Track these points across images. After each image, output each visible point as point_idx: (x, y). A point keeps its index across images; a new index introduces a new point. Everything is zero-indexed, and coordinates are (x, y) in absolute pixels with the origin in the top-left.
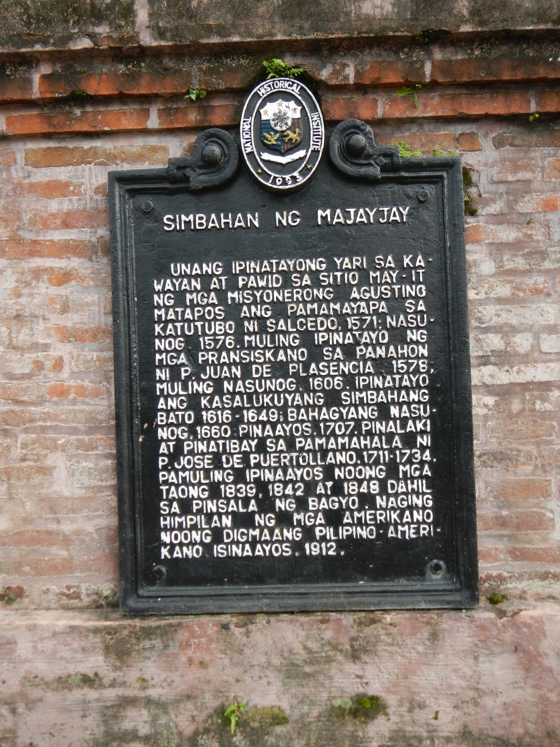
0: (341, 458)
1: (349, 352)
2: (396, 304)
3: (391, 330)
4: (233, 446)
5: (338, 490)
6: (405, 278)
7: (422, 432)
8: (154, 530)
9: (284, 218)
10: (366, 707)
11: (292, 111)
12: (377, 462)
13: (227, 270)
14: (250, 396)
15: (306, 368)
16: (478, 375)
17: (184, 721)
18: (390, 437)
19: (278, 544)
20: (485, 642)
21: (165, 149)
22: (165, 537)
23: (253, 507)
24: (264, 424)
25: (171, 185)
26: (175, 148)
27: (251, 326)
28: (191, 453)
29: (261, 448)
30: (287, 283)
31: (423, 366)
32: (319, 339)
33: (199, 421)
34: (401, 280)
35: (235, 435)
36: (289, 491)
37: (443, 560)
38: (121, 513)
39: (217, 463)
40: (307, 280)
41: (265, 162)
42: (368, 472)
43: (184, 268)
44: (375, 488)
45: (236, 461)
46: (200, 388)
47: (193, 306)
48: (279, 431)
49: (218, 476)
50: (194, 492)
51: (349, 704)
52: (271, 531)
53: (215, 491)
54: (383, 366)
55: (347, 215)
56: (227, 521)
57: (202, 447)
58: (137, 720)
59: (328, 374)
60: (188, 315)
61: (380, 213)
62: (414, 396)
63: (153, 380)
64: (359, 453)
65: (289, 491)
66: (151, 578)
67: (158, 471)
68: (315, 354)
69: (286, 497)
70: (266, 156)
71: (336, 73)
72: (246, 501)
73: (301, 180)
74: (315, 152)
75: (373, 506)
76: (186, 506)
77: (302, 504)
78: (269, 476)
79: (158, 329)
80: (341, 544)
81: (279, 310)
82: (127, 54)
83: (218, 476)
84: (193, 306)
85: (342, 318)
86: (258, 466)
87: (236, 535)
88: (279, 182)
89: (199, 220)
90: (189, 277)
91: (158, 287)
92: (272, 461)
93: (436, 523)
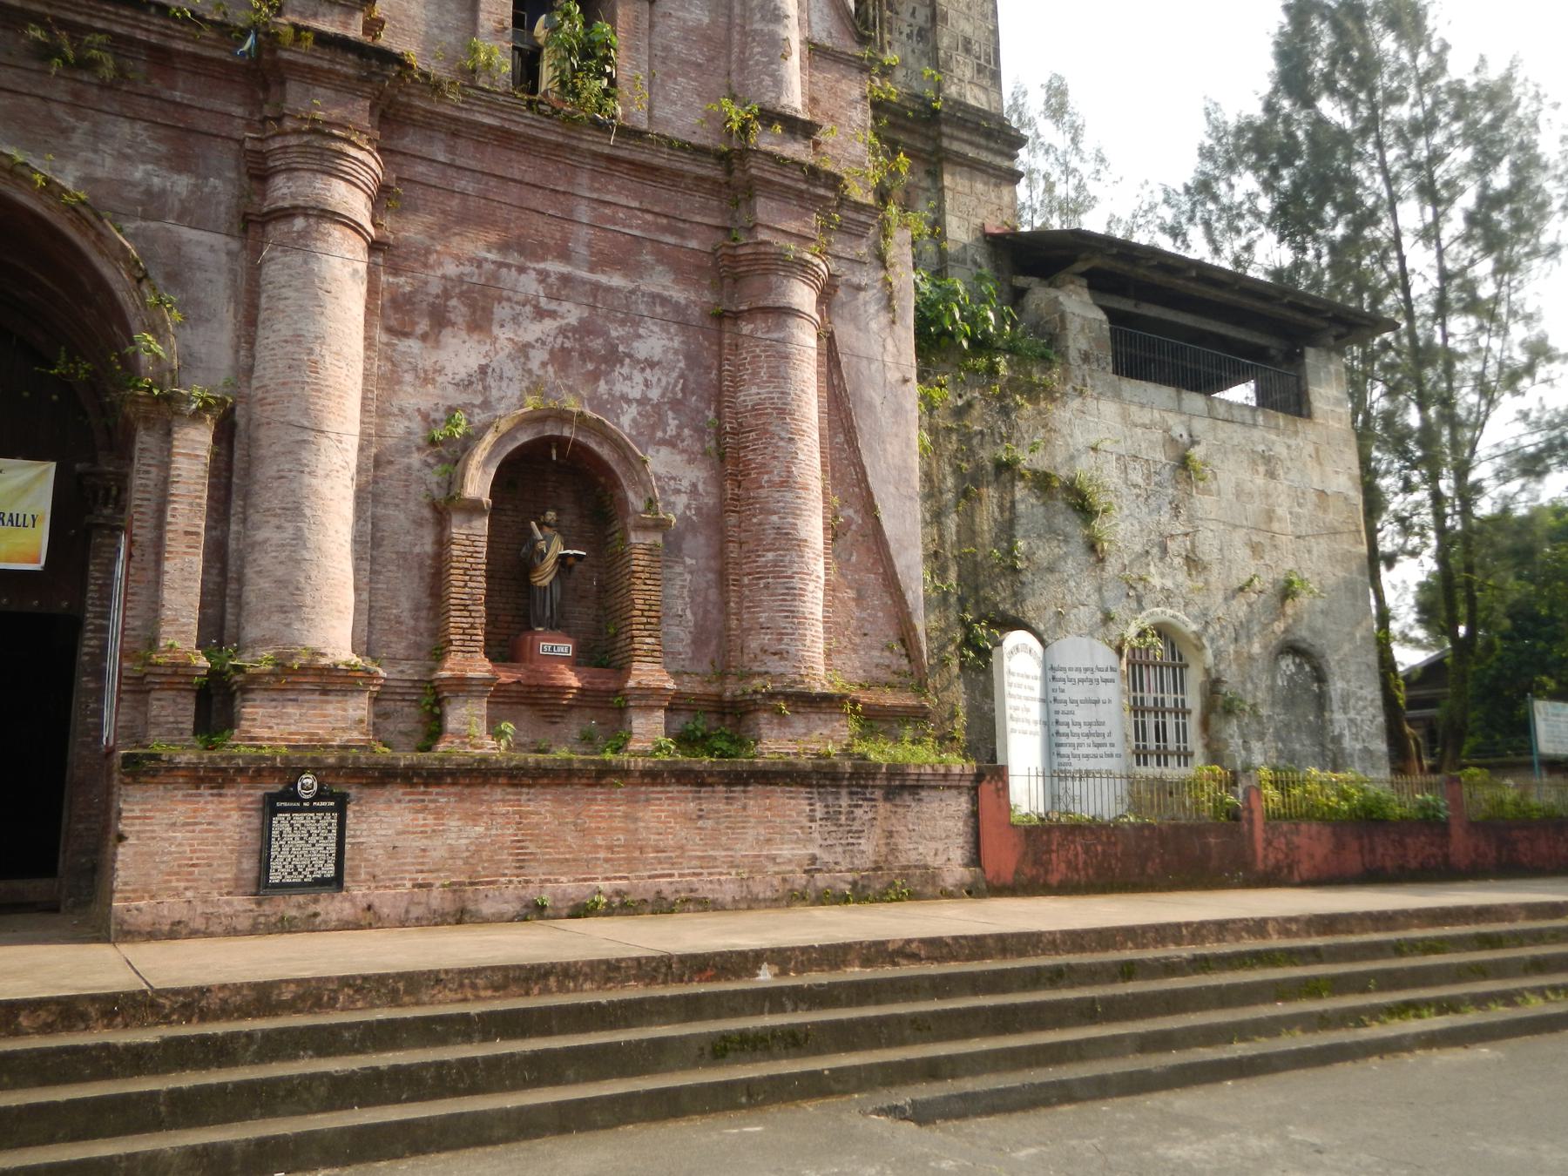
10: (316, 915)
17: (273, 920)
20: (345, 899)
25: (281, 796)
26: (280, 787)
37: (336, 883)
58: (262, 919)
59: (313, 840)
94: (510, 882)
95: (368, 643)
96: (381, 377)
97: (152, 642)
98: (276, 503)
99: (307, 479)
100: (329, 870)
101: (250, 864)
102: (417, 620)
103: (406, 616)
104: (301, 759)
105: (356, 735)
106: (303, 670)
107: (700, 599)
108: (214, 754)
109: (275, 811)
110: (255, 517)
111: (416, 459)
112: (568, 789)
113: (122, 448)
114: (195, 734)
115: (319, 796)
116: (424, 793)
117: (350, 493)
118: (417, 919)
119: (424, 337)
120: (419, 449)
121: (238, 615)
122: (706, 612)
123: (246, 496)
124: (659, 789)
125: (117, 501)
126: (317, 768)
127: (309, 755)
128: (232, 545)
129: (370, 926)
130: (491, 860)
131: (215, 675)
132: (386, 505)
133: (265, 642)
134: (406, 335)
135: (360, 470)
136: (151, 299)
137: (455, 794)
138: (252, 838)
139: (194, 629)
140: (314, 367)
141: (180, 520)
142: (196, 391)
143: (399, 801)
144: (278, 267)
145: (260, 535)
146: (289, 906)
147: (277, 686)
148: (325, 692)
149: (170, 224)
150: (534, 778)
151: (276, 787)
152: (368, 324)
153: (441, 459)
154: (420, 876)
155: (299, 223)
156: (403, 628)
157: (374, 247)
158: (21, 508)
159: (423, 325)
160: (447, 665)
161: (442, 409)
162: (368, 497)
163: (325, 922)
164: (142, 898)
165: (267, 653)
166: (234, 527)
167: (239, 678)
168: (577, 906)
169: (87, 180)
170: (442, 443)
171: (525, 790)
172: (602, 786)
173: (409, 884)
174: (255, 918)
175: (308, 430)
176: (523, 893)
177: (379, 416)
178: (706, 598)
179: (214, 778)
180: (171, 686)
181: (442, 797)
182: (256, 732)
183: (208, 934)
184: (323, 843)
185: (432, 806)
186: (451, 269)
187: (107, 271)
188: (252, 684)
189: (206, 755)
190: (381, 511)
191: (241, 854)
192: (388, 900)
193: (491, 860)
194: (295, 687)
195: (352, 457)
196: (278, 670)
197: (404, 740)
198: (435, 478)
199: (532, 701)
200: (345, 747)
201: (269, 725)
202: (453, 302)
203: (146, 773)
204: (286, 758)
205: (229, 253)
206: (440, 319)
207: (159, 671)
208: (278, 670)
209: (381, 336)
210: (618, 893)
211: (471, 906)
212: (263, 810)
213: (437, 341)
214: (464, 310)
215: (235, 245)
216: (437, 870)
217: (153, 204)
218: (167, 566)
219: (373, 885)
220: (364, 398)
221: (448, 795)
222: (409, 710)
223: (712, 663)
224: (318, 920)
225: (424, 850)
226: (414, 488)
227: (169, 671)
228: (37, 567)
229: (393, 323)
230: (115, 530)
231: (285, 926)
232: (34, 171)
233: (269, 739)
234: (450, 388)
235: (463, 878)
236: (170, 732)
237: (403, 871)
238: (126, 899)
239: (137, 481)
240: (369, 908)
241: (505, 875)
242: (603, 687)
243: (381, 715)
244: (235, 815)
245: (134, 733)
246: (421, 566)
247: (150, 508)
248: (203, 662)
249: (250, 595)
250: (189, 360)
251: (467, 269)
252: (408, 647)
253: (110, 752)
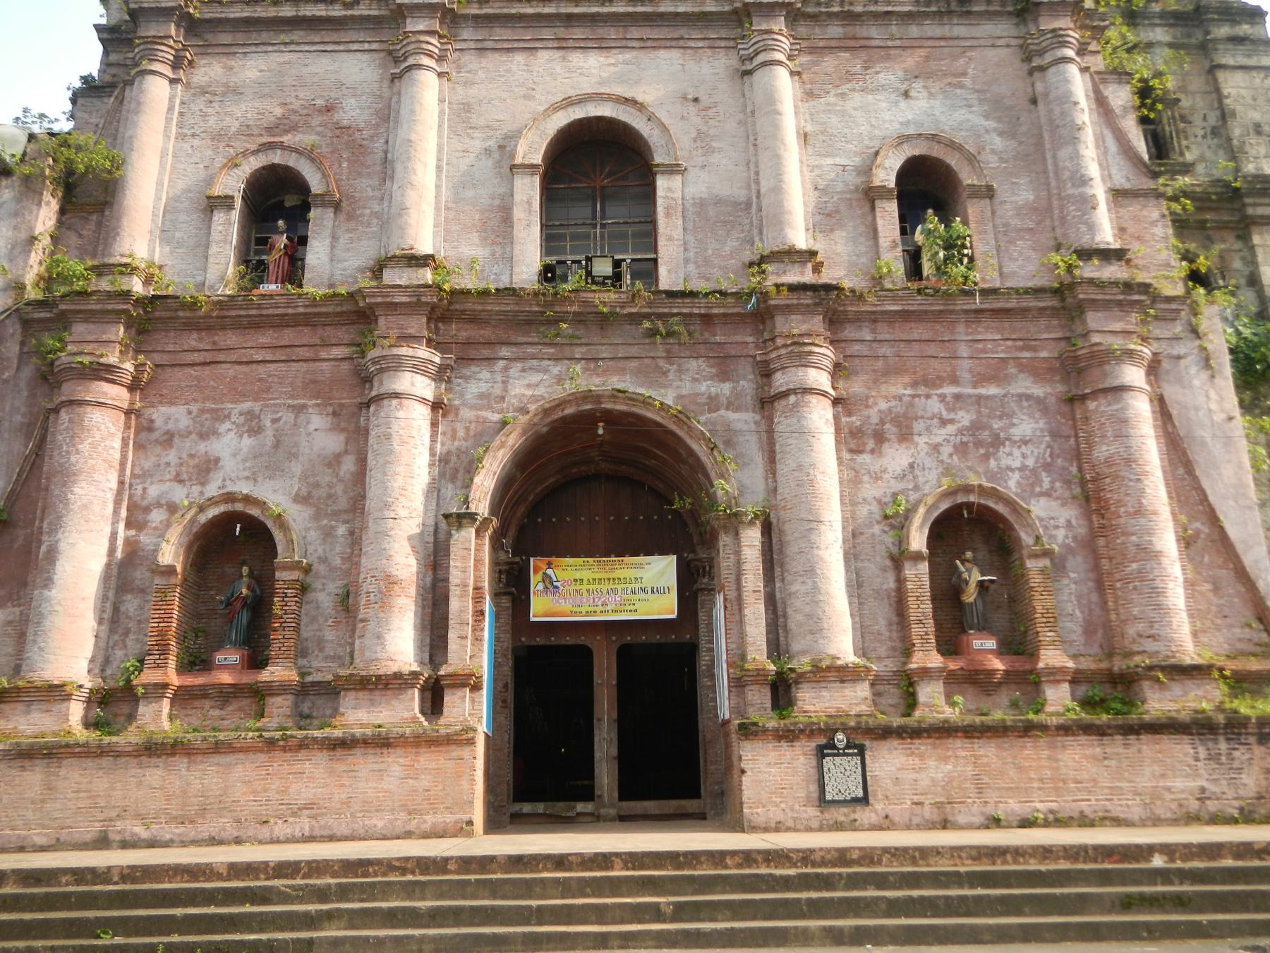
10: (855, 820)
19: (841, 798)
37: (864, 800)
59: (848, 773)
82: (820, 729)
95: (863, 649)
96: (850, 481)
97: (743, 657)
98: (800, 568)
99: (815, 551)
100: (860, 794)
101: (814, 788)
102: (890, 631)
103: (884, 630)
105: (864, 708)
106: (829, 668)
107: (1084, 602)
108: (787, 722)
109: (824, 756)
110: (788, 578)
111: (877, 529)
113: (710, 541)
115: (848, 747)
117: (841, 557)
119: (872, 451)
120: (878, 522)
121: (786, 637)
122: (1091, 610)
123: (782, 565)
125: (709, 574)
126: (845, 729)
127: (839, 721)
128: (778, 595)
129: (888, 829)
130: (959, 787)
131: (779, 674)
132: (862, 561)
133: (804, 652)
134: (861, 452)
135: (844, 541)
136: (720, 459)
138: (813, 772)
139: (764, 647)
140: (812, 483)
141: (750, 584)
142: (749, 507)
144: (782, 424)
145: (794, 588)
146: (840, 814)
148: (842, 681)
149: (722, 412)
150: (981, 732)
151: (823, 741)
152: (838, 451)
153: (892, 527)
155: (792, 399)
157: (836, 402)
158: (661, 583)
159: (871, 444)
160: (914, 660)
161: (889, 495)
162: (851, 556)
165: (806, 659)
166: (777, 585)
167: (793, 675)
169: (680, 397)
170: (892, 517)
175: (813, 522)
177: (852, 505)
179: (788, 736)
180: (756, 682)
181: (922, 745)
182: (807, 708)
183: (796, 830)
184: (854, 776)
186: (883, 405)
187: (695, 447)
188: (801, 678)
189: (782, 722)
190: (860, 565)
191: (808, 781)
192: (898, 812)
193: (959, 787)
194: (824, 680)
195: (838, 534)
197: (893, 710)
198: (890, 540)
199: (973, 680)
200: (859, 716)
201: (815, 703)
202: (887, 426)
204: (826, 723)
205: (755, 423)
206: (880, 438)
209: (846, 456)
210: (1052, 812)
211: (950, 818)
213: (880, 453)
214: (894, 430)
215: (758, 417)
217: (713, 403)
218: (746, 612)
220: (841, 496)
222: (893, 690)
223: (1101, 646)
224: (857, 824)
226: (878, 547)
228: (674, 616)
229: (853, 446)
230: (711, 591)
231: (838, 827)
232: (654, 400)
234: (892, 481)
235: (942, 799)
236: (759, 709)
239: (724, 564)
240: (887, 817)
243: (877, 694)
244: (802, 758)
245: (738, 710)
246: (889, 597)
247: (732, 578)
248: (772, 667)
249: (792, 625)
250: (742, 489)
251: (893, 403)
253: (726, 723)
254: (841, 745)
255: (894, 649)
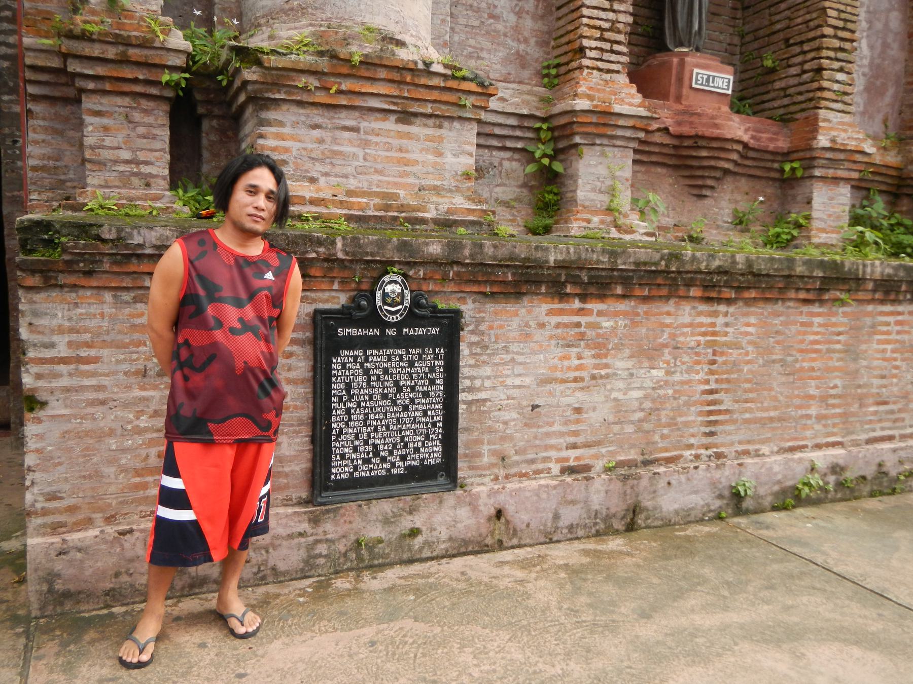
0: (408, 433)
1: (413, 389)
2: (432, 369)
3: (430, 379)
4: (364, 430)
5: (406, 446)
6: (436, 358)
7: (439, 421)
8: (329, 467)
9: (390, 332)
10: (414, 533)
11: (398, 288)
12: (421, 434)
13: (365, 353)
14: (372, 408)
15: (395, 396)
16: (462, 396)
17: (341, 547)
18: (427, 423)
20: (459, 502)
21: (339, 298)
22: (333, 471)
23: (371, 455)
24: (377, 420)
25: (345, 316)
27: (373, 378)
28: (346, 433)
29: (376, 430)
30: (389, 360)
31: (441, 394)
32: (401, 383)
33: (350, 419)
34: (434, 359)
35: (365, 425)
36: (386, 448)
37: (444, 473)
38: (313, 461)
39: (357, 437)
40: (397, 359)
41: (386, 310)
42: (418, 438)
43: (346, 352)
44: (420, 444)
45: (365, 436)
46: (351, 405)
47: (349, 369)
48: (383, 423)
49: (357, 443)
50: (346, 450)
51: (408, 532)
52: (378, 465)
53: (355, 449)
54: (426, 395)
55: (415, 331)
56: (360, 462)
57: (351, 431)
58: (322, 549)
59: (404, 398)
60: (347, 373)
61: (428, 331)
62: (437, 407)
63: (331, 402)
64: (415, 430)
65: (386, 448)
66: (327, 489)
67: (331, 442)
68: (399, 389)
69: (384, 450)
70: (386, 307)
71: (416, 273)
72: (368, 453)
73: (400, 318)
74: (406, 307)
75: (419, 452)
76: (343, 456)
77: (391, 453)
78: (378, 442)
79: (334, 379)
80: (406, 468)
81: (386, 371)
82: (330, 260)
83: (357, 443)
84: (349, 369)
85: (411, 375)
86: (374, 438)
87: (364, 468)
88: (391, 319)
89: (354, 332)
90: (348, 356)
91: (334, 361)
92: (380, 435)
93: (442, 458)
94: (697, 457)
100: (433, 453)
102: (519, 14)
104: (380, 245)
105: (460, 202)
107: (879, 26)
112: (779, 307)
114: (173, 186)
115: (412, 318)
116: (580, 312)
118: (571, 528)
122: (885, 46)
124: (888, 308)
129: (501, 546)
130: (672, 424)
137: (625, 314)
143: (542, 326)
146: (371, 520)
147: (321, 97)
148: (406, 117)
150: (739, 289)
154: (573, 454)
156: (500, 27)
160: (581, 89)
163: (428, 544)
164: (88, 523)
167: (250, 74)
168: (784, 492)
171: (722, 308)
172: (822, 302)
173: (556, 468)
174: (311, 547)
176: (717, 474)
178: (886, 25)
180: (115, 87)
181: (607, 317)
185: (590, 333)
188: (278, 86)
192: (531, 498)
193: (672, 424)
196: (324, 64)
199: (683, 159)
203: (69, 267)
207: (96, 50)
208: (324, 64)
210: (836, 469)
211: (647, 503)
212: (314, 342)
216: (598, 443)
219: (502, 473)
221: (616, 314)
223: (885, 122)
224: (419, 541)
225: (578, 411)
227: (111, 52)
233: (313, 202)
235: (633, 455)
237: (547, 448)
238: (55, 528)
240: (499, 514)
241: (690, 447)
242: (771, 147)
252: (506, 61)
254: (393, 314)
255: (521, 60)
